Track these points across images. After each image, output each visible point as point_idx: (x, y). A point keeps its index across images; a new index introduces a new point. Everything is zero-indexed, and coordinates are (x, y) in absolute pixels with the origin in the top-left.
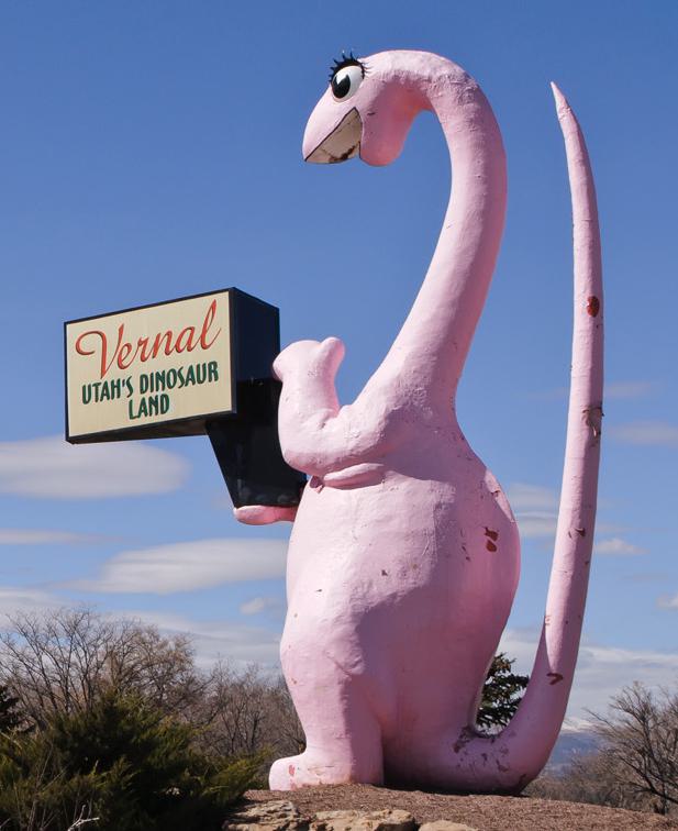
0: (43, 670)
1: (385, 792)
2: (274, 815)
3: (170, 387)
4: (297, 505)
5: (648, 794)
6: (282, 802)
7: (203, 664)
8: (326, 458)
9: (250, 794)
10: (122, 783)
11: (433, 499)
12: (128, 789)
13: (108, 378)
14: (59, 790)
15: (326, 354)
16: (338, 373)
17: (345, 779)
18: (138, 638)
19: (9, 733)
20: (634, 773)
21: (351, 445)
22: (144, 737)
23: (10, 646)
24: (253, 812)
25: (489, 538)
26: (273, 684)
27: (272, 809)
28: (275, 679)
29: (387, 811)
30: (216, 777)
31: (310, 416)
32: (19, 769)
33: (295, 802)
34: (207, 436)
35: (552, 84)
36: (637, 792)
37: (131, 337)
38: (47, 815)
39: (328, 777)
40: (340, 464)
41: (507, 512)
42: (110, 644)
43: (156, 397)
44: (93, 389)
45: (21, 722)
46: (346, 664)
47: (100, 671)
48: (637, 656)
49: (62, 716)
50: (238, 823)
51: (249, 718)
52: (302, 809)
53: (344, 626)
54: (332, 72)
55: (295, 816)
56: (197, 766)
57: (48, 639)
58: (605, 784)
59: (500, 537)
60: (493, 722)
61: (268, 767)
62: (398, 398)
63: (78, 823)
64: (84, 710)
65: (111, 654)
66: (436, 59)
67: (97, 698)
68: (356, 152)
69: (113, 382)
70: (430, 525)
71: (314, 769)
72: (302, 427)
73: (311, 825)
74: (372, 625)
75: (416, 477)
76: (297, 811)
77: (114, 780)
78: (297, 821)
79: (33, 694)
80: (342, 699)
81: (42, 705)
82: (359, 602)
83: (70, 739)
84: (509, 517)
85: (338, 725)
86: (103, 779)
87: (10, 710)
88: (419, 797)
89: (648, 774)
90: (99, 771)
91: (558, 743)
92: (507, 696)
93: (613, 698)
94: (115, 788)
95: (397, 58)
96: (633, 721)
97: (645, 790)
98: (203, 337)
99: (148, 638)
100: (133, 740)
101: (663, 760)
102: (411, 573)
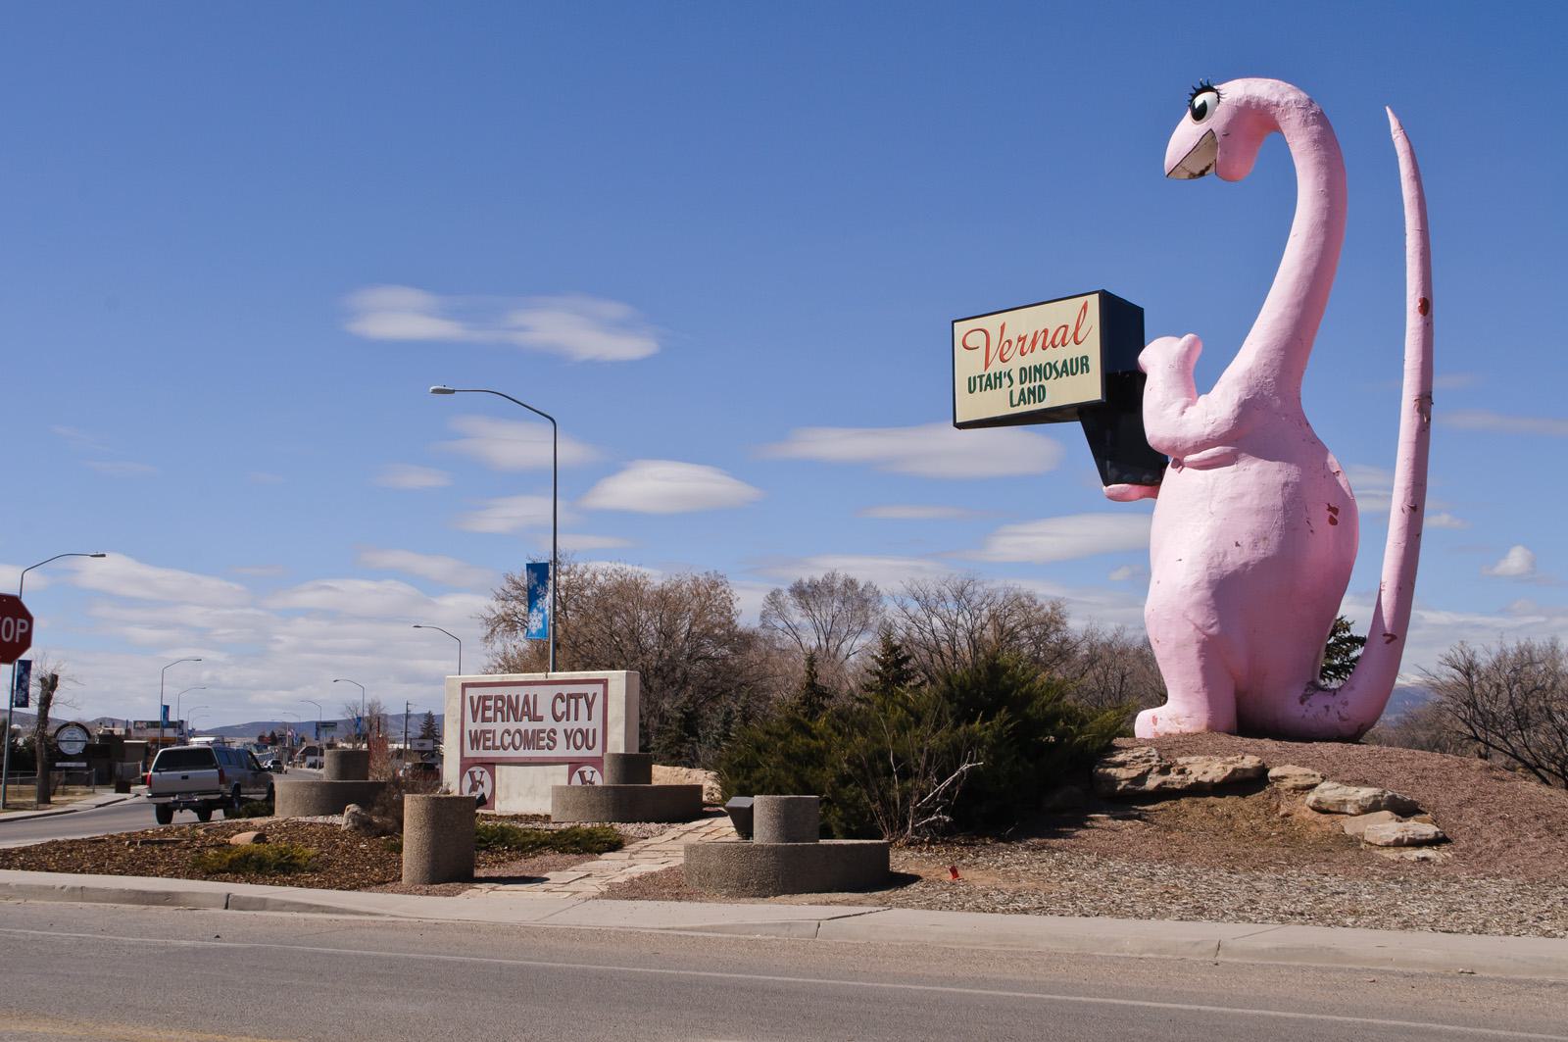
0: (933, 631)
1: (1238, 740)
2: (1139, 760)
3: (1047, 379)
4: (1160, 483)
5: (1472, 741)
6: (1146, 749)
7: (1076, 626)
8: (1186, 442)
9: (1118, 741)
10: (1004, 732)
11: (1281, 478)
12: (1009, 737)
13: (991, 370)
14: (948, 738)
15: (1186, 349)
16: (1197, 365)
17: (1202, 728)
18: (1018, 603)
19: (902, 687)
20: (1460, 722)
21: (1208, 430)
22: (1024, 690)
23: (904, 609)
24: (1120, 758)
25: (1330, 513)
26: (1138, 643)
27: (1137, 754)
28: (1140, 639)
29: (1240, 756)
30: (1087, 726)
31: (1172, 404)
32: (912, 719)
33: (1157, 749)
34: (1079, 423)
35: (1388, 110)
36: (1463, 739)
37: (1011, 334)
38: (937, 760)
39: (1187, 726)
40: (1199, 447)
41: (1347, 490)
42: (993, 607)
43: (1034, 387)
44: (978, 380)
45: (913, 677)
46: (1203, 625)
47: (984, 632)
48: (1462, 619)
49: (950, 672)
50: (1107, 767)
51: (1117, 674)
52: (1164, 755)
53: (1201, 592)
54: (1191, 98)
55: (1158, 761)
56: (1071, 716)
57: (938, 603)
58: (1434, 732)
59: (1340, 512)
60: (1334, 677)
61: (1134, 717)
62: (1250, 389)
63: (965, 767)
64: (970, 667)
65: (993, 617)
66: (1283, 86)
67: (982, 656)
68: (1212, 169)
69: (995, 374)
70: (1278, 501)
71: (1175, 719)
72: (1164, 414)
73: (1172, 769)
74: (1226, 591)
75: (1266, 459)
76: (1160, 756)
77: (996, 729)
78: (1160, 766)
79: (924, 652)
80: (1200, 657)
81: (932, 662)
82: (1215, 571)
83: (957, 693)
84: (1349, 494)
85: (1196, 680)
86: (986, 729)
87: (904, 667)
88: (1269, 744)
89: (1473, 724)
90: (982, 722)
91: (1392, 696)
92: (1347, 654)
93: (1441, 656)
94: (997, 736)
95: (1249, 84)
96: (1459, 676)
97: (1470, 737)
98: (1075, 334)
99: (1027, 603)
100: (1013, 694)
101: (1487, 711)
102: (1261, 544)
